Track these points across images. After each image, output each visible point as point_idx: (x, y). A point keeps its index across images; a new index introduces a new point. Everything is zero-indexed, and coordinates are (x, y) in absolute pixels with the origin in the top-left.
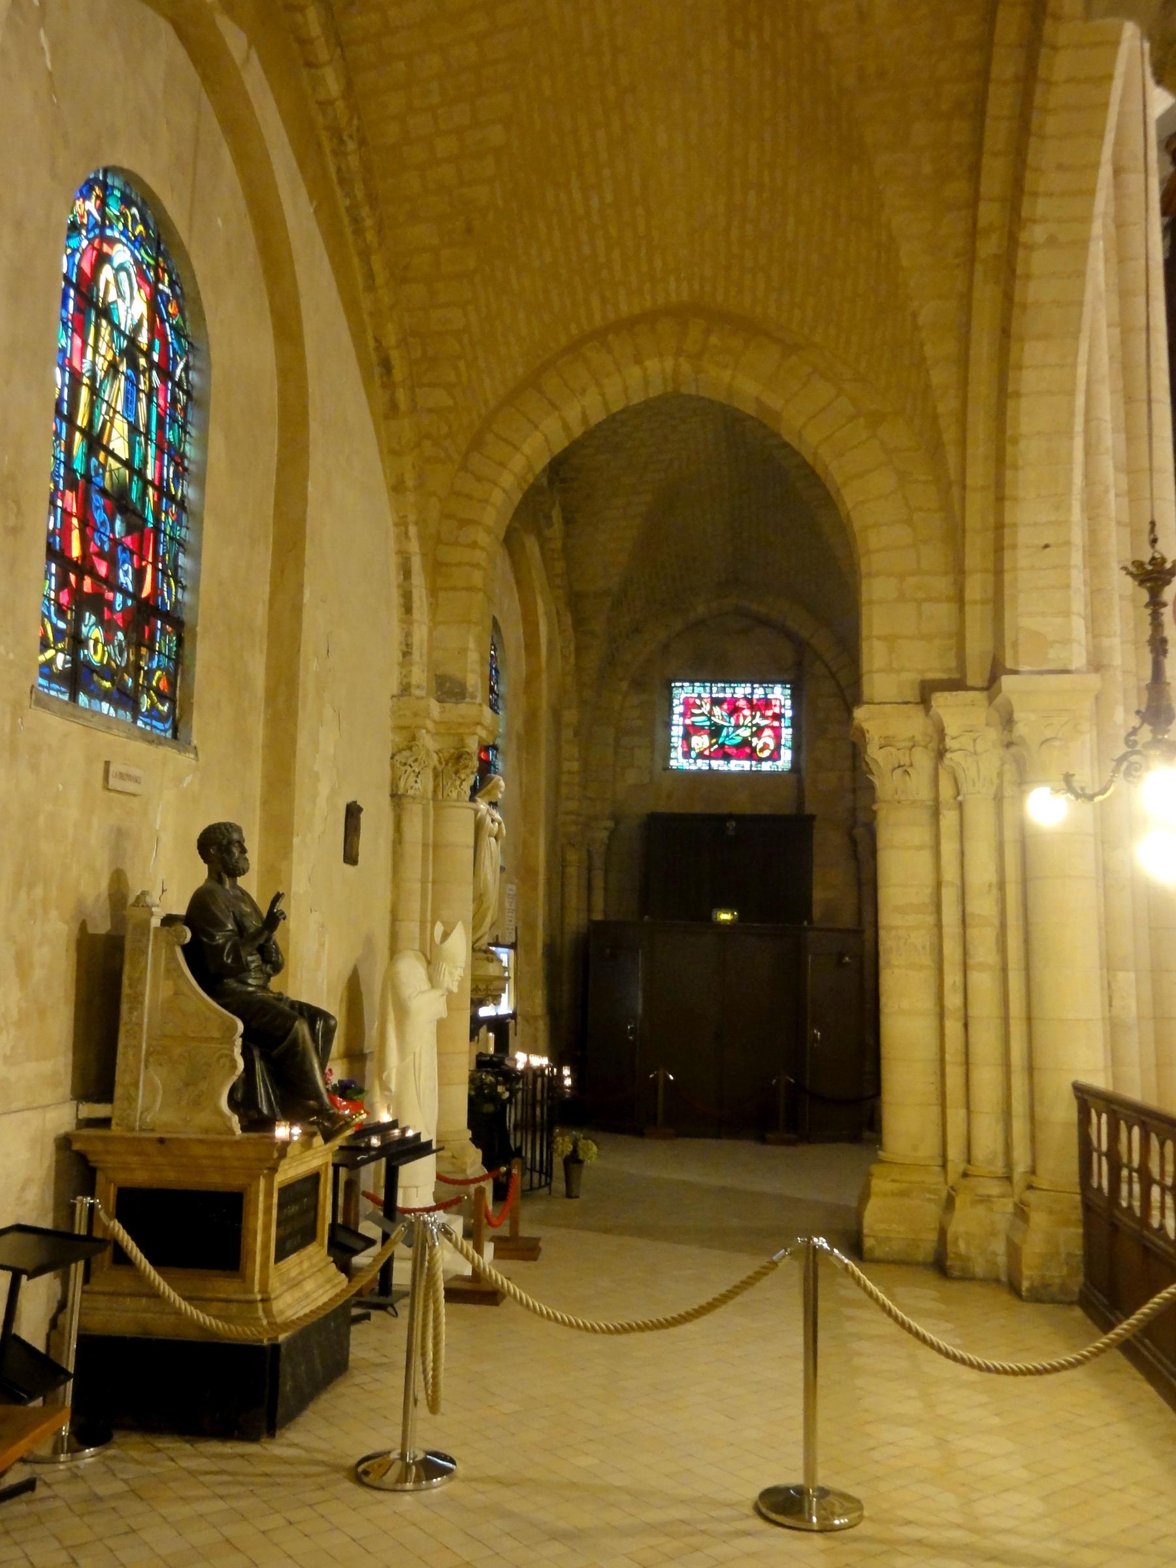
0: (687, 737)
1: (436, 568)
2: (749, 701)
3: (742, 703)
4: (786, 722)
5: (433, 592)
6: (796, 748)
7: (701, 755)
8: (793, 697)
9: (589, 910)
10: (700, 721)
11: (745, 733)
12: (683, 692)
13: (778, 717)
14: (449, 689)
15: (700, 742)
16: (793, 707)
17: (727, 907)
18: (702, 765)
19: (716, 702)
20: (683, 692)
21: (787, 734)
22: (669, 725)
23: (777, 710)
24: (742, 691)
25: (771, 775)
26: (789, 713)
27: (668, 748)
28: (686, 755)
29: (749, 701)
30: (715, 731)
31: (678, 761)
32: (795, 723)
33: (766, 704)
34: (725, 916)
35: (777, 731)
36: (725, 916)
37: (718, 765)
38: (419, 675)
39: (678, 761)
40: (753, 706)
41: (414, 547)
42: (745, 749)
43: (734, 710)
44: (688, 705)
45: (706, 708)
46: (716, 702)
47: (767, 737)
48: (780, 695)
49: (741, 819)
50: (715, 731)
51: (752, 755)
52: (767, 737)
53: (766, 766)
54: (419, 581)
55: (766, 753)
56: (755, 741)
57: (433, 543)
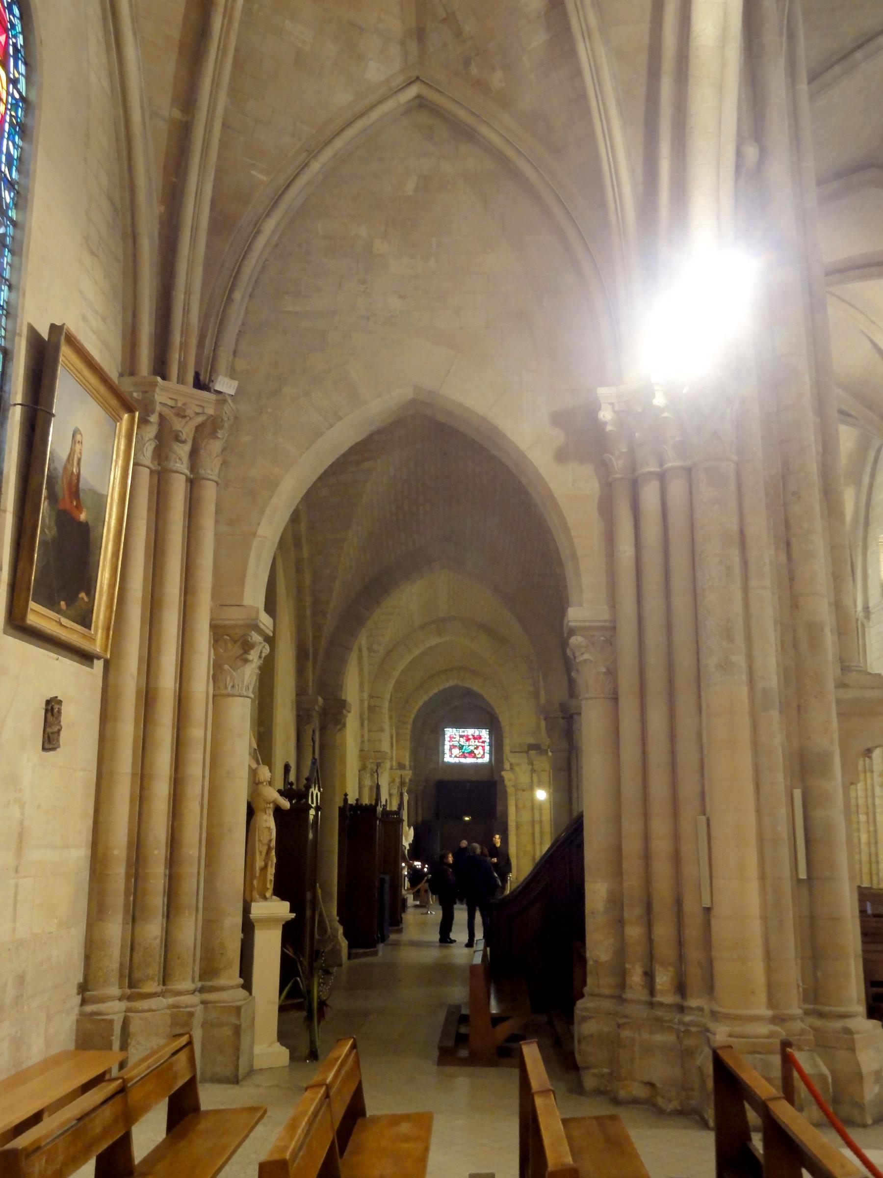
0: (450, 750)
1: (398, 734)
2: (473, 736)
3: (471, 737)
4: (486, 744)
5: (397, 741)
6: (490, 754)
7: (456, 757)
8: (490, 734)
9: (417, 815)
10: (456, 744)
11: (472, 748)
12: (449, 732)
13: (483, 742)
14: (401, 766)
15: (456, 751)
16: (490, 738)
17: (467, 816)
18: (457, 760)
19: (461, 736)
20: (449, 732)
21: (487, 748)
22: (444, 745)
23: (483, 739)
24: (470, 732)
25: (483, 765)
26: (488, 740)
27: (444, 754)
28: (451, 756)
29: (473, 736)
30: (461, 747)
31: (447, 759)
32: (490, 745)
33: (480, 737)
34: (467, 819)
35: (484, 750)
36: (467, 819)
37: (463, 760)
38: (394, 763)
39: (447, 759)
40: (475, 738)
41: (394, 731)
42: (472, 754)
43: (468, 740)
44: (451, 738)
45: (458, 739)
46: (461, 736)
47: (480, 750)
48: (485, 734)
49: (470, 782)
50: (461, 747)
51: (475, 756)
52: (480, 750)
53: (480, 761)
54: (394, 739)
55: (480, 756)
56: (476, 751)
57: (397, 728)
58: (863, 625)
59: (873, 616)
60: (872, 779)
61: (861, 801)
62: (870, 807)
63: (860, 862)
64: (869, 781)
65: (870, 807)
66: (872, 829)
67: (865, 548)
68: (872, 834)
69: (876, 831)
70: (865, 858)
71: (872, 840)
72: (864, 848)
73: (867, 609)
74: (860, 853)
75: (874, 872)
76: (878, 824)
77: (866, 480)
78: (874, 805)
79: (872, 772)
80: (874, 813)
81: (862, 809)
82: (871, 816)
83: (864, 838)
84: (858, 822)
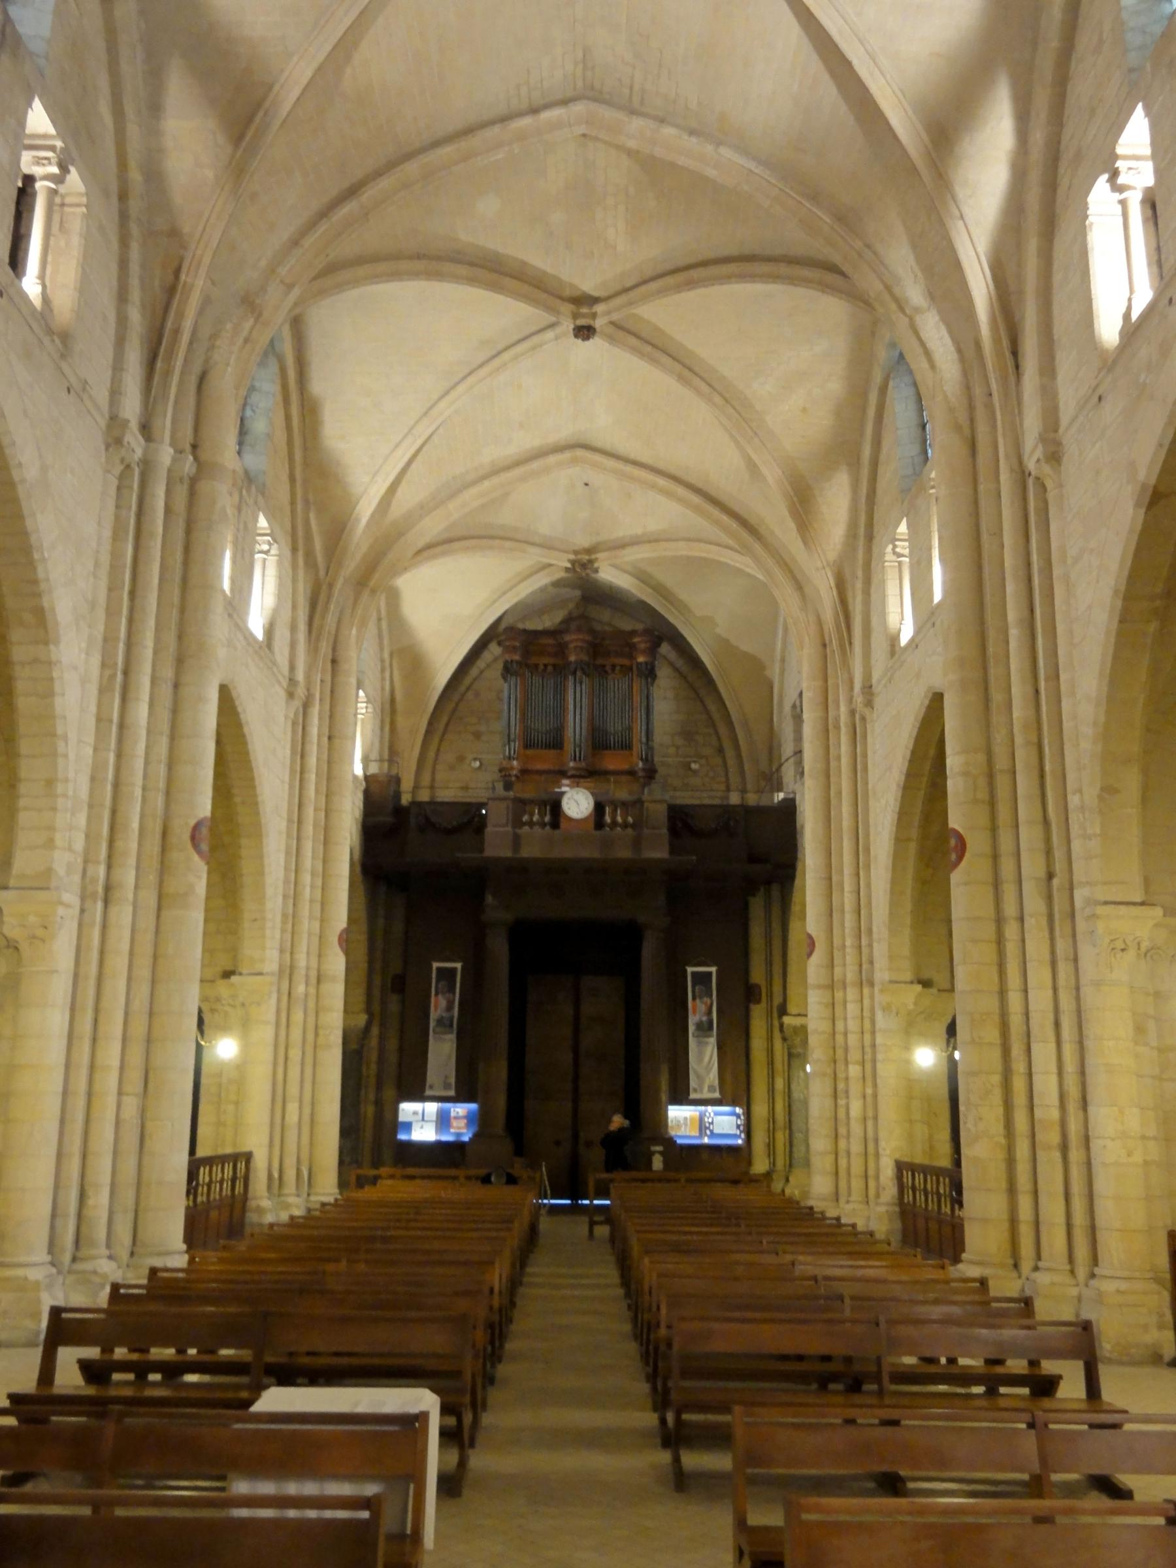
58: (863, 719)
59: (878, 701)
60: (872, 997)
61: (853, 1040)
62: (868, 1050)
63: (848, 1153)
64: (866, 1002)
65: (868, 1050)
66: (869, 1091)
67: (868, 581)
68: (869, 1099)
69: (875, 1096)
70: (856, 1147)
71: (870, 1114)
72: (856, 1129)
73: (868, 688)
74: (848, 1136)
75: (871, 1173)
76: (878, 1081)
77: (867, 452)
78: (874, 1046)
79: (871, 984)
80: (874, 1061)
81: (854, 1055)
82: (868, 1066)
83: (856, 1108)
84: (847, 1079)
